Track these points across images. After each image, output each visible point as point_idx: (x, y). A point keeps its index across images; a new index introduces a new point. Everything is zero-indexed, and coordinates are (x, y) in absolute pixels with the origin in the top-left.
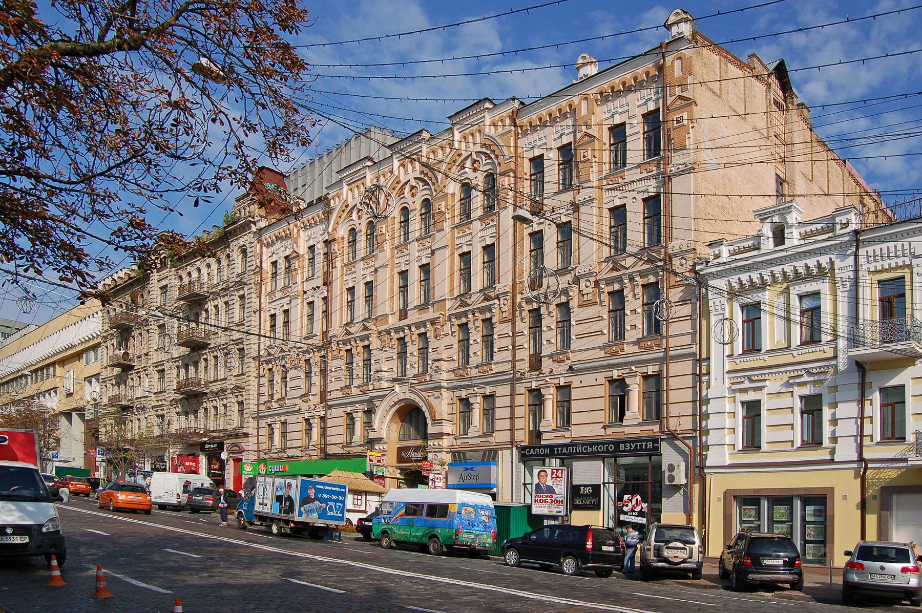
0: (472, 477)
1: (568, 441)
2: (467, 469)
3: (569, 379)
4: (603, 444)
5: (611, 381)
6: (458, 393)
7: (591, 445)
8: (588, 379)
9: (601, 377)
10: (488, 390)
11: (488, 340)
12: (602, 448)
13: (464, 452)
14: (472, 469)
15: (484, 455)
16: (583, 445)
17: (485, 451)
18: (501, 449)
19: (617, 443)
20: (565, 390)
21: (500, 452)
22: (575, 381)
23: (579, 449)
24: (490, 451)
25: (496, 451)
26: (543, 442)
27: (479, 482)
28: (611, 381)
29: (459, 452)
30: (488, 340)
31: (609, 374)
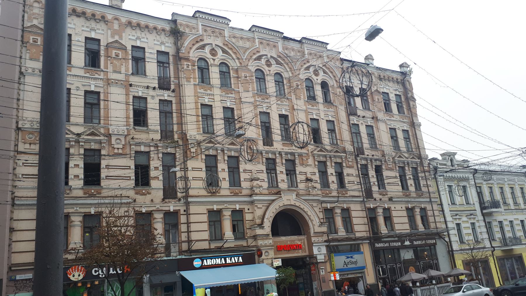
0: (352, 263)
2: (348, 257)
3: (390, 206)
5: (407, 209)
6: (324, 205)
8: (398, 207)
9: (404, 206)
10: (345, 206)
13: (337, 246)
14: (352, 257)
21: (361, 246)
22: (393, 207)
24: (355, 245)
27: (358, 265)
28: (407, 209)
29: (333, 246)
31: (407, 206)
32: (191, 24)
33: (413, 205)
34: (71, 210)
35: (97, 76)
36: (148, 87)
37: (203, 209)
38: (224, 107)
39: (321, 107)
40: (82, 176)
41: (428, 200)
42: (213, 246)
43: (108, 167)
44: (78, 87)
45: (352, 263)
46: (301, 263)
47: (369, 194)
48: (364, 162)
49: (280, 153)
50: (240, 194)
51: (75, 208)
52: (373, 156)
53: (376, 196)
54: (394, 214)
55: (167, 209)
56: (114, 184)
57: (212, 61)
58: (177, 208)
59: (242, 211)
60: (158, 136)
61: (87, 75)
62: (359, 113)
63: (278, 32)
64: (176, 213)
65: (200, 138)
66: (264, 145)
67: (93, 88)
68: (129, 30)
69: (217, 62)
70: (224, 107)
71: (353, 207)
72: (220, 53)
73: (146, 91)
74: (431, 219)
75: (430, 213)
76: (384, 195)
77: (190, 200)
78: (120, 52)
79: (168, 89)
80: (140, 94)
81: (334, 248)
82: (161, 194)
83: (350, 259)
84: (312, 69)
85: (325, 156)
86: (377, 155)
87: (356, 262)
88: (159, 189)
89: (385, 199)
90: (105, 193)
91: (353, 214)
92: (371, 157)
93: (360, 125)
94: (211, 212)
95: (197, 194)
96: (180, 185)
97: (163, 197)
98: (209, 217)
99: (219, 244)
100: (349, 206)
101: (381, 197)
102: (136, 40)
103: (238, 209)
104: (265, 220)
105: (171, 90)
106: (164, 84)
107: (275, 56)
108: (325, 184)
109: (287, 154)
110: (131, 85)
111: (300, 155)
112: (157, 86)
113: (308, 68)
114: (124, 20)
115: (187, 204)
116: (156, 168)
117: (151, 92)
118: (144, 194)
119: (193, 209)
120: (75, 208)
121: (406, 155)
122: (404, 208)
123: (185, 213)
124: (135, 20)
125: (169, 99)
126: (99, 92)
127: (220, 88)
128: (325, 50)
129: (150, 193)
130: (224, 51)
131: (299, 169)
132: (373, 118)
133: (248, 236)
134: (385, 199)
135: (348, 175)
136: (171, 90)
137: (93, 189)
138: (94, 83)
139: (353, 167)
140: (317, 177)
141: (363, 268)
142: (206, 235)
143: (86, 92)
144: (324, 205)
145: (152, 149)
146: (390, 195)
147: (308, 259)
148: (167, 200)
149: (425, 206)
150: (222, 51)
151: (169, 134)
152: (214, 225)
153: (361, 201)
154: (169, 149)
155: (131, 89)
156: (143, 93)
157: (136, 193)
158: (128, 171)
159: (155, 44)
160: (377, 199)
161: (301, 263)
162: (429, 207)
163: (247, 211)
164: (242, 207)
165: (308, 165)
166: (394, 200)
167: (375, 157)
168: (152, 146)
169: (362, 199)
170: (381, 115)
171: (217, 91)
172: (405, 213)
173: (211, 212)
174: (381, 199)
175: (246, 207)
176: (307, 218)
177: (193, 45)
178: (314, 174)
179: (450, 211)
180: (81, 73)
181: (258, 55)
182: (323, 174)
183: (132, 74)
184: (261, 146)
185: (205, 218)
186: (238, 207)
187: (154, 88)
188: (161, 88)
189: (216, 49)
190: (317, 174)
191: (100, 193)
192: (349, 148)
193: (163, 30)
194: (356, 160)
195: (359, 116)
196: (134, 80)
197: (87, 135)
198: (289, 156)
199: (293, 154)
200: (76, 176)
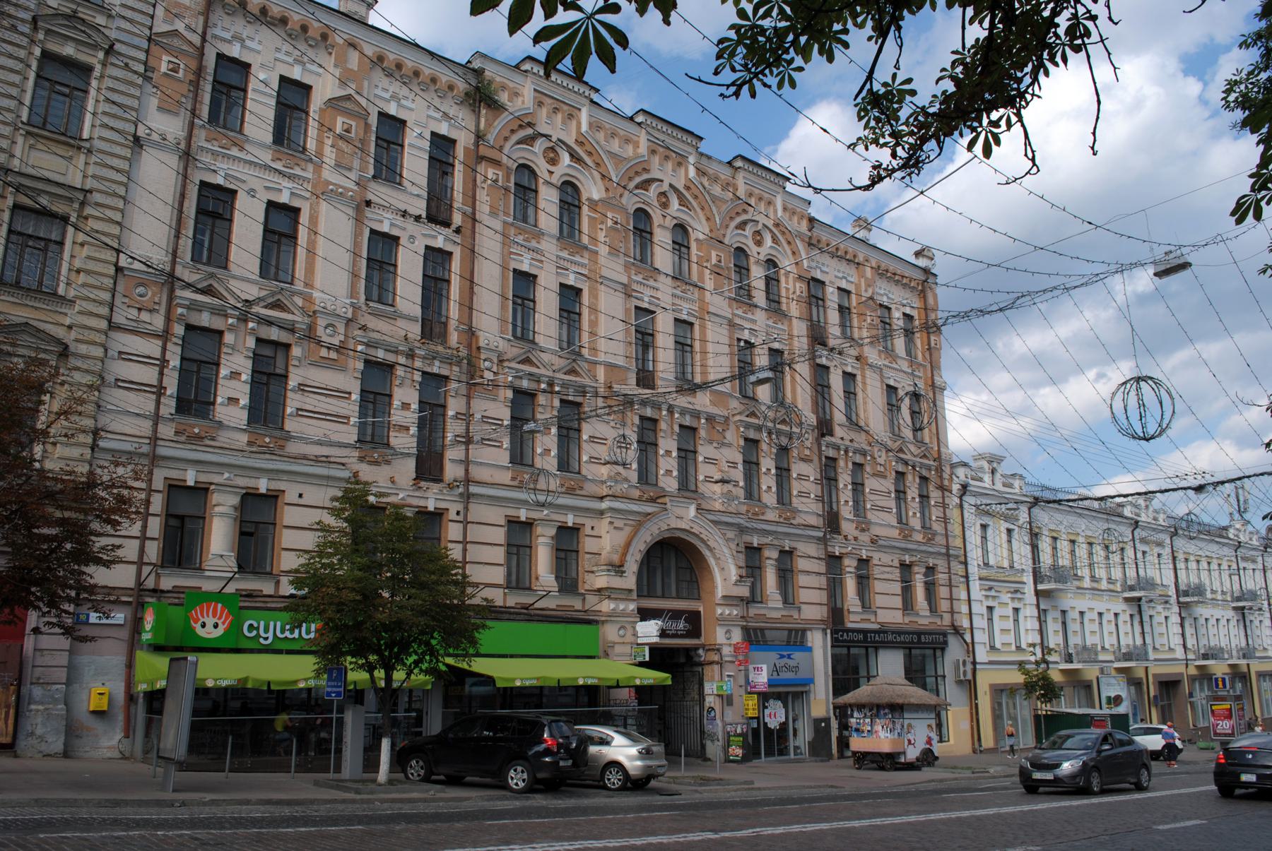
0: (789, 669)
1: (876, 627)
2: (782, 657)
4: (909, 633)
6: (747, 538)
7: (900, 633)
8: (886, 558)
11: (783, 473)
12: (908, 638)
13: (762, 630)
14: (789, 657)
15: (789, 636)
16: (893, 633)
17: (790, 630)
18: (810, 629)
19: (919, 634)
20: (864, 563)
21: (809, 633)
22: (877, 557)
23: (890, 638)
24: (797, 631)
25: (804, 631)
26: (850, 625)
29: (755, 629)
30: (783, 473)
32: (511, 85)
33: (914, 559)
34: (216, 479)
35: (297, 171)
36: (404, 214)
37: (497, 515)
38: (561, 284)
39: (760, 316)
40: (245, 401)
41: (944, 551)
42: (511, 602)
43: (302, 388)
44: (253, 190)
45: (789, 669)
46: (682, 660)
47: (832, 522)
48: (831, 453)
49: (671, 410)
50: (578, 492)
51: (226, 475)
52: (851, 441)
53: (847, 527)
54: (876, 572)
55: (422, 503)
56: (314, 429)
57: (546, 176)
58: (442, 505)
59: (578, 529)
60: (415, 330)
61: (278, 166)
62: (832, 342)
63: (691, 133)
64: (438, 515)
65: (502, 345)
66: (638, 385)
67: (284, 198)
68: (378, 76)
69: (555, 179)
70: (561, 284)
71: (804, 548)
72: (566, 159)
73: (399, 221)
74: (943, 592)
75: (941, 577)
76: (863, 530)
77: (473, 489)
78: (354, 124)
79: (447, 224)
80: (385, 228)
81: (756, 634)
82: (411, 464)
83: (785, 660)
84: (749, 231)
85: (759, 428)
86: (861, 441)
87: (796, 669)
88: (408, 455)
89: (865, 538)
90: (293, 448)
91: (802, 564)
92: (848, 443)
93: (832, 369)
94: (513, 523)
95: (489, 480)
96: (453, 453)
97: (414, 475)
98: (509, 534)
99: (526, 599)
100: (794, 544)
101: (856, 533)
102: (388, 101)
103: (570, 524)
104: (628, 558)
105: (454, 227)
106: (437, 214)
107: (681, 187)
108: (751, 492)
109: (683, 412)
110: (368, 203)
111: (710, 419)
112: (424, 215)
113: (741, 226)
114: (369, 51)
115: (467, 498)
116: (405, 406)
117: (411, 226)
118: (376, 463)
119: (478, 511)
120: (226, 475)
121: (913, 448)
122: (896, 563)
123: (460, 518)
124: (393, 53)
125: (449, 248)
126: (299, 210)
127: (558, 239)
128: (781, 190)
129: (388, 462)
130: (574, 157)
131: (704, 451)
132: (858, 359)
133: (587, 587)
134: (865, 538)
135: (801, 477)
136: (454, 227)
137: (270, 437)
138: (290, 185)
139: (811, 461)
140: (738, 474)
141: (810, 681)
142: (498, 575)
143: (271, 204)
144: (747, 538)
145: (402, 360)
146: (876, 531)
147: (701, 652)
148: (423, 484)
149: (936, 562)
150: (571, 155)
151: (437, 330)
152: (518, 554)
153: (819, 539)
154: (437, 363)
155: (368, 212)
156: (392, 225)
157: (361, 459)
158: (343, 403)
159: (429, 116)
160: (850, 537)
161: (682, 660)
162: (941, 564)
163: (588, 531)
164: (580, 520)
165: (723, 444)
166: (880, 542)
167: (856, 445)
168: (402, 353)
169: (821, 534)
170: (872, 354)
171: (549, 246)
172: (896, 574)
173: (513, 523)
174: (856, 539)
175: (588, 523)
176: (712, 562)
177: (513, 131)
178: (733, 465)
179: (980, 579)
180: (266, 157)
181: (645, 176)
182: (751, 466)
183: (374, 177)
184: (630, 386)
185: (499, 535)
186: (570, 520)
187: (417, 218)
188: (432, 219)
189: (558, 149)
190: (740, 467)
191: (282, 447)
192: (811, 419)
193: (451, 88)
194: (819, 445)
195: (832, 350)
196: (379, 192)
197: (266, 307)
198: (688, 417)
199: (696, 415)
200: (233, 401)
